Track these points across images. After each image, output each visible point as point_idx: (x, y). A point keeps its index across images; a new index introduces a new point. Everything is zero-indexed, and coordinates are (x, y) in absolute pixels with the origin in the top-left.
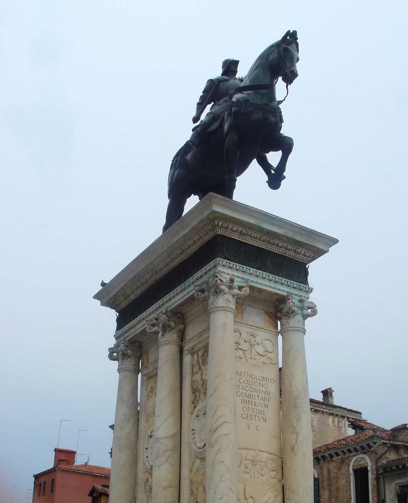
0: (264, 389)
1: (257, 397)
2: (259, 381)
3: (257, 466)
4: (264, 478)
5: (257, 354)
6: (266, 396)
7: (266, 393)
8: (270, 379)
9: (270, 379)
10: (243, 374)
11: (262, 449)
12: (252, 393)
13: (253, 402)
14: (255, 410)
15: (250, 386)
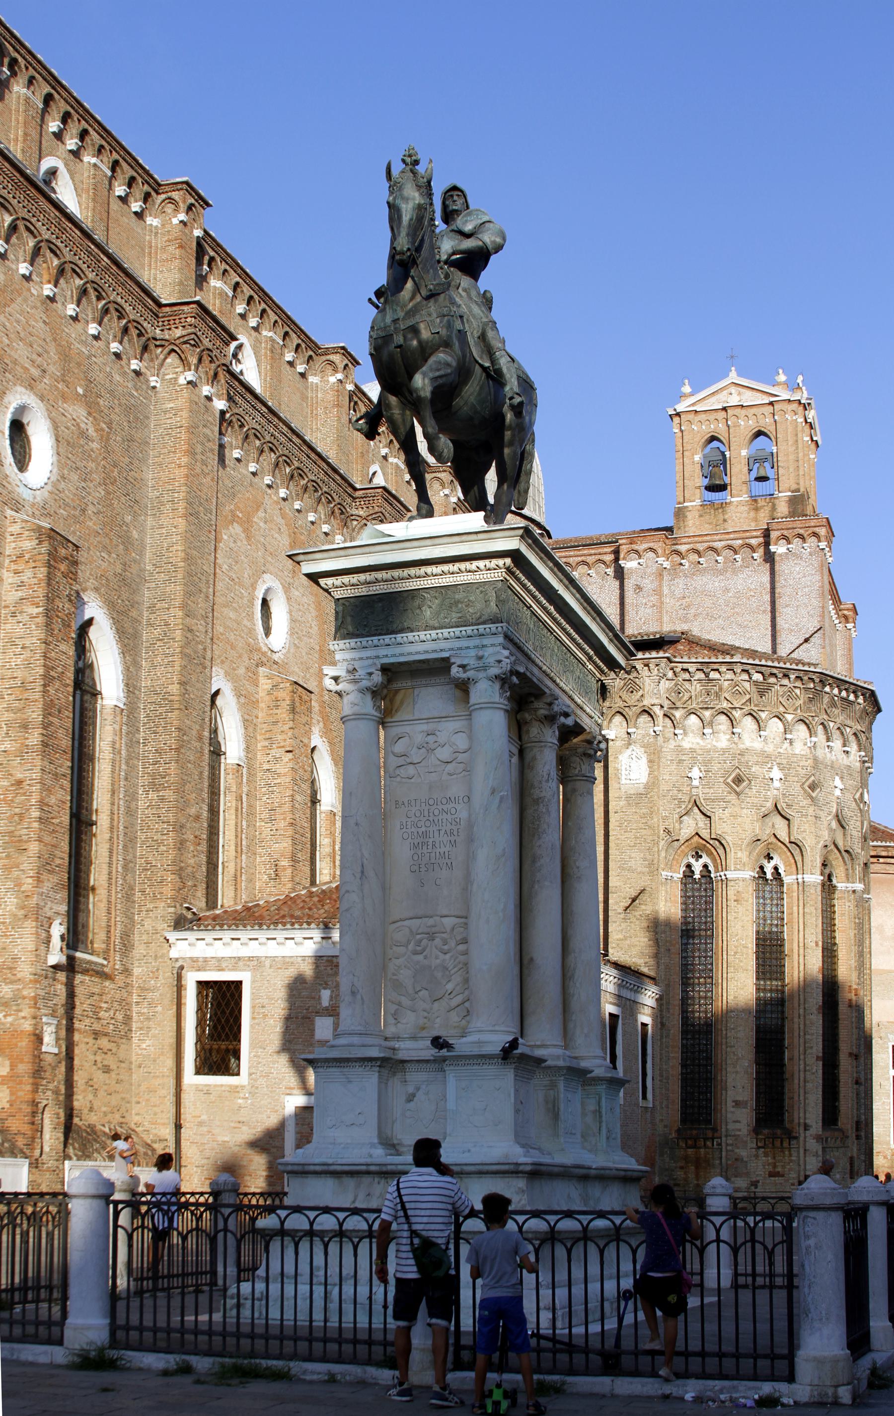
0: (449, 817)
1: (436, 834)
2: (440, 807)
3: (438, 941)
4: (448, 956)
5: (439, 763)
6: (453, 827)
7: (454, 823)
8: (461, 798)
9: (461, 798)
10: (413, 802)
11: (445, 912)
12: (428, 829)
13: (430, 844)
14: (433, 855)
15: (425, 819)
